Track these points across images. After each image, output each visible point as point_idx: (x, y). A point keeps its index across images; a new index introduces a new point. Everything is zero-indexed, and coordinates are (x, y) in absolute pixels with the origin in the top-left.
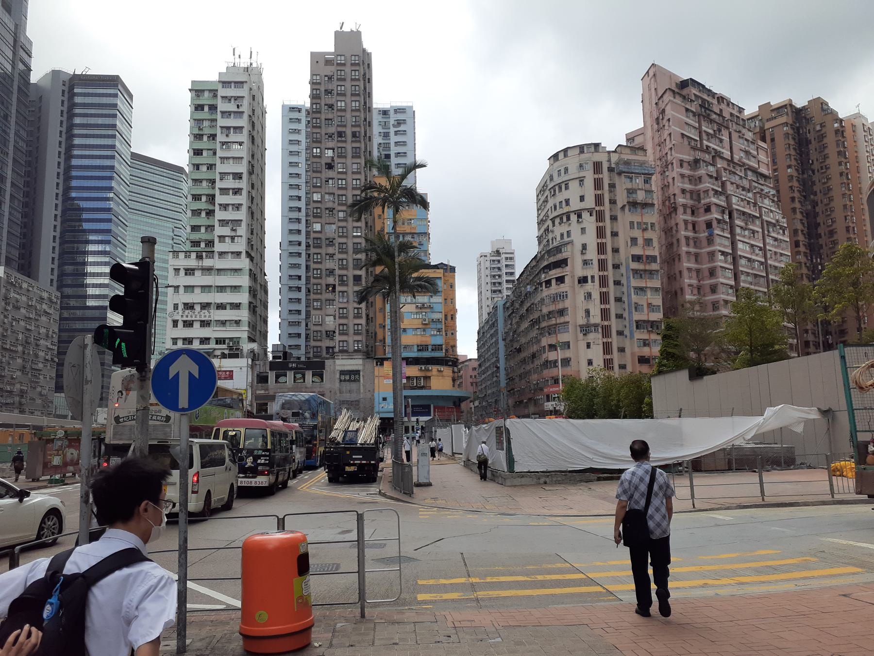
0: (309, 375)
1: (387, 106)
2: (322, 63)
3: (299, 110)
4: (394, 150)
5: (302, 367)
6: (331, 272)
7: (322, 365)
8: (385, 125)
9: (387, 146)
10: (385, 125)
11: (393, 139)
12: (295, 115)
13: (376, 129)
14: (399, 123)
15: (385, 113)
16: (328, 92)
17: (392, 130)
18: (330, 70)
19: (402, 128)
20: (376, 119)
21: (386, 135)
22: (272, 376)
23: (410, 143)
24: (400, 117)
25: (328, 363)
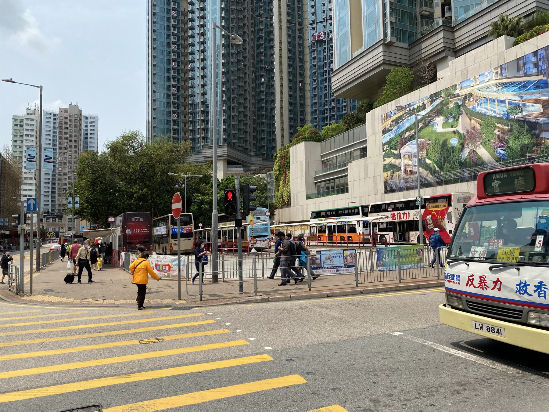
0: (57, 219)
1: (87, 115)
2: (63, 112)
3: (51, 114)
4: (89, 132)
5: (55, 217)
6: (65, 184)
7: (62, 216)
8: (86, 122)
9: (87, 130)
10: (86, 122)
11: (89, 128)
12: (49, 116)
13: (83, 124)
14: (92, 122)
15: (86, 118)
16: (66, 123)
17: (89, 125)
18: (66, 115)
19: (93, 124)
20: (83, 119)
21: (87, 126)
22: (44, 219)
23: (96, 134)
24: (92, 120)
25: (64, 216)
